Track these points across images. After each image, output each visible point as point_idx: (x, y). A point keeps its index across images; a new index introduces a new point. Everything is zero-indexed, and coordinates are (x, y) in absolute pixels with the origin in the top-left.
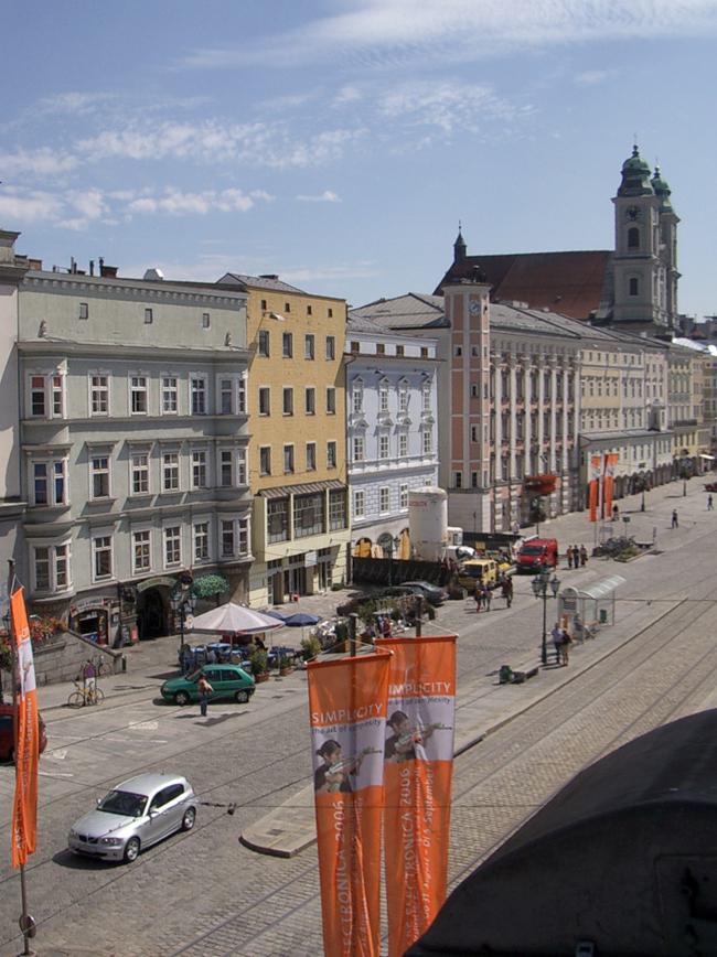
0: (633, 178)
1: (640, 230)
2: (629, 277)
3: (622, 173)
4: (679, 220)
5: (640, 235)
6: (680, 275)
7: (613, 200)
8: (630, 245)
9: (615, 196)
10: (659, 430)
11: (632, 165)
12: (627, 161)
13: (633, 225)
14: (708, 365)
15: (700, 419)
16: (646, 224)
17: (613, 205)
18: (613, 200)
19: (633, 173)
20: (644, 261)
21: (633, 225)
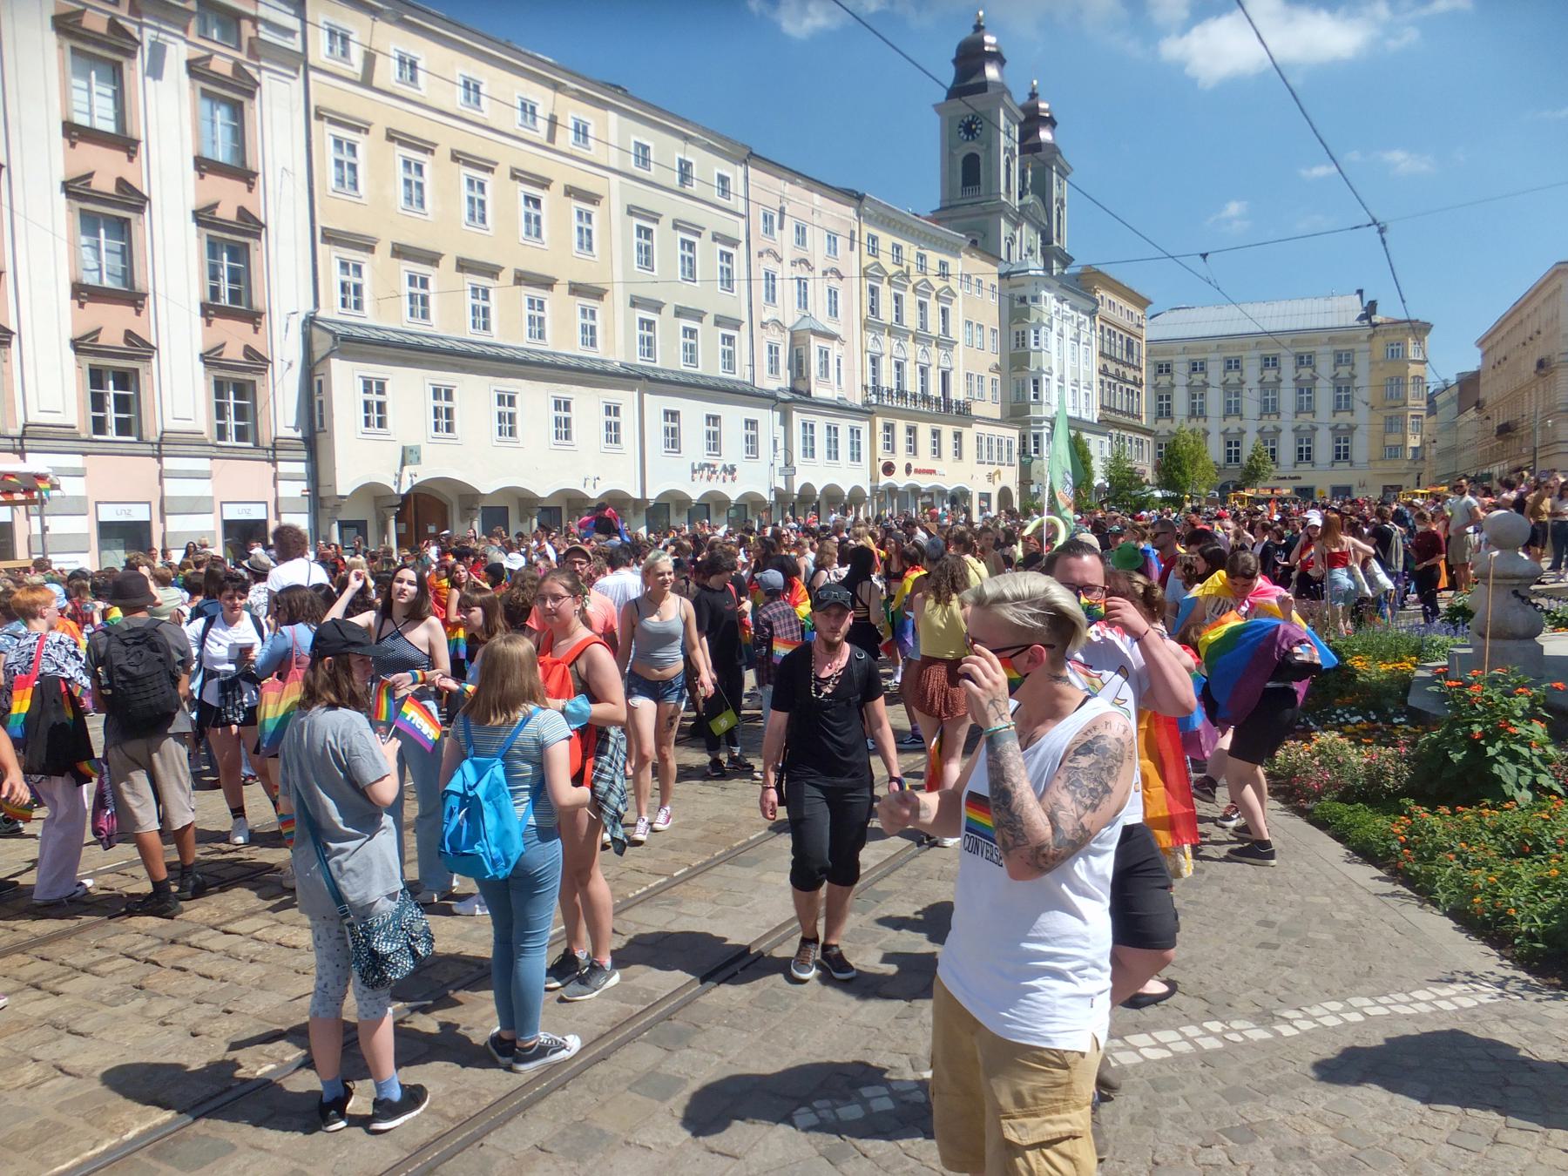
1: (982, 155)
3: (955, 62)
8: (965, 184)
10: (809, 394)
13: (971, 147)
15: (988, 407)
16: (991, 145)
17: (938, 118)
18: (938, 108)
19: (971, 57)
21: (971, 147)
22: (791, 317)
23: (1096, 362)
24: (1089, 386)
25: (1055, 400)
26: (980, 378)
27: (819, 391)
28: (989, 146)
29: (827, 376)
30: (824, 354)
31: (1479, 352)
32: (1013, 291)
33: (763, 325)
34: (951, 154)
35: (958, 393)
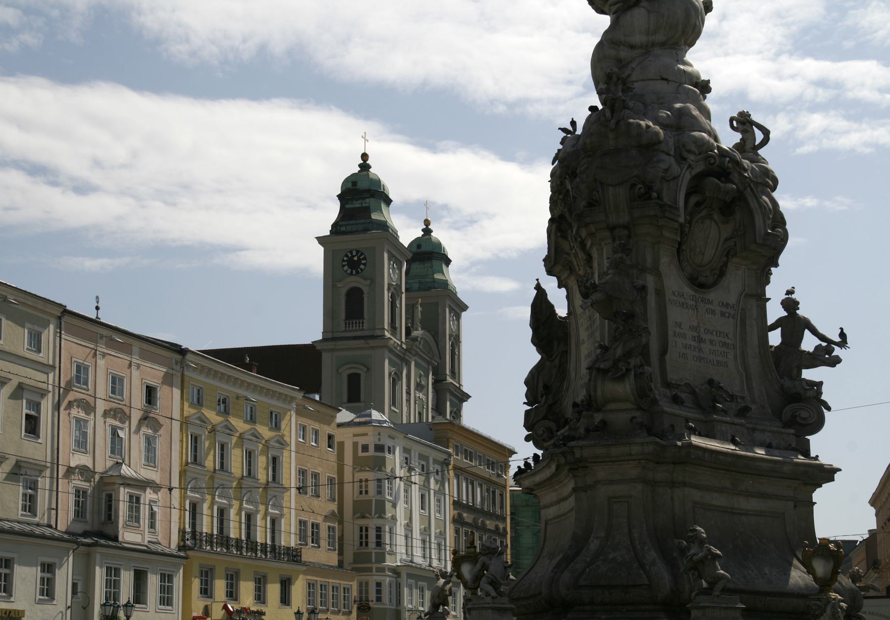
0: (357, 204)
1: (366, 290)
2: (346, 372)
4: (465, 308)
5: (365, 296)
6: (467, 397)
7: (321, 240)
8: (349, 316)
9: (326, 231)
10: (116, 539)
11: (354, 183)
12: (346, 180)
13: (354, 281)
14: (365, 448)
16: (375, 280)
17: (320, 250)
18: (321, 240)
20: (372, 343)
21: (354, 281)
22: (102, 463)
23: (450, 512)
24: (442, 535)
25: (401, 549)
26: (315, 526)
27: (128, 536)
28: (373, 281)
29: (138, 520)
30: (135, 501)
31: (873, 511)
32: (356, 439)
33: (70, 471)
34: (334, 286)
35: (289, 539)
